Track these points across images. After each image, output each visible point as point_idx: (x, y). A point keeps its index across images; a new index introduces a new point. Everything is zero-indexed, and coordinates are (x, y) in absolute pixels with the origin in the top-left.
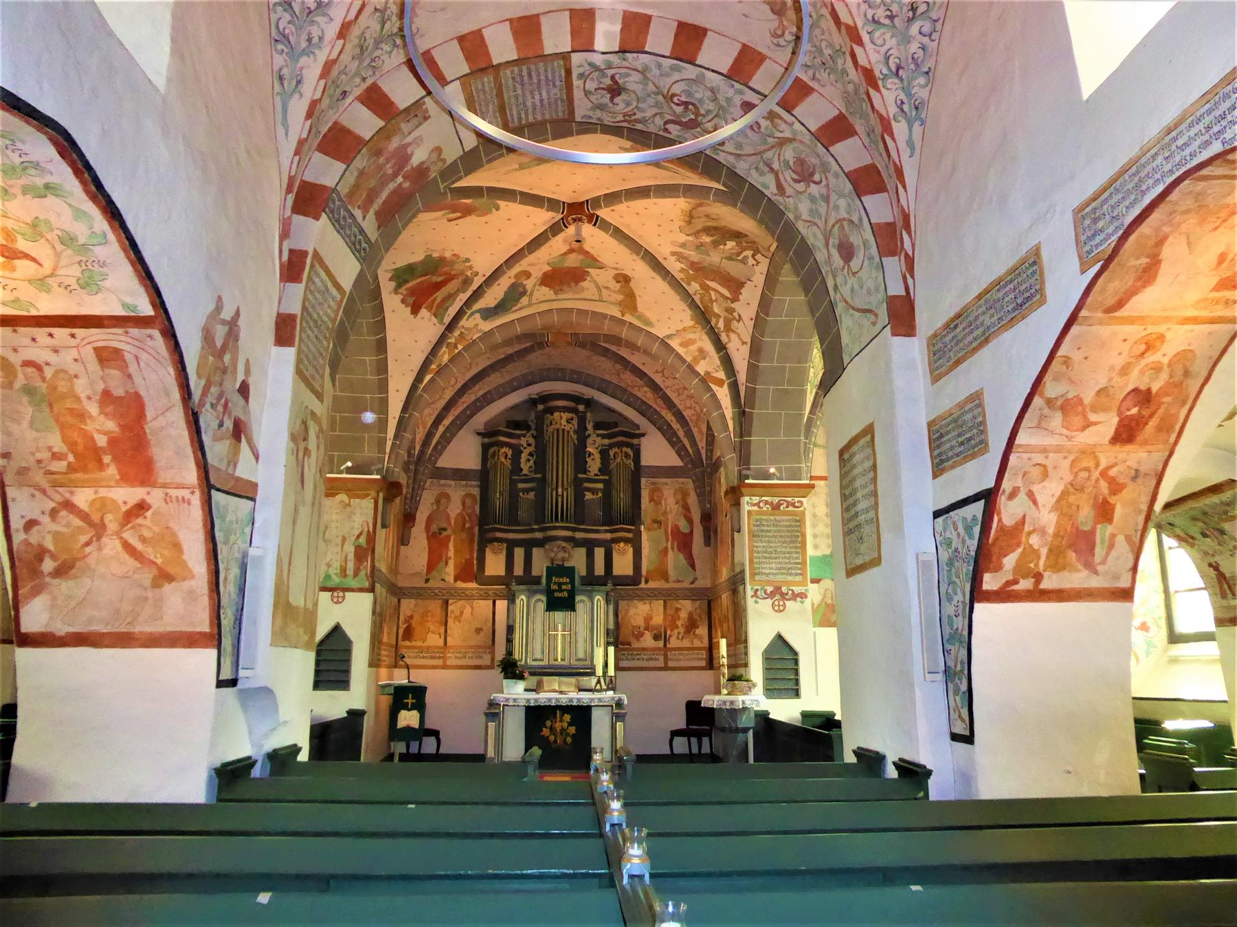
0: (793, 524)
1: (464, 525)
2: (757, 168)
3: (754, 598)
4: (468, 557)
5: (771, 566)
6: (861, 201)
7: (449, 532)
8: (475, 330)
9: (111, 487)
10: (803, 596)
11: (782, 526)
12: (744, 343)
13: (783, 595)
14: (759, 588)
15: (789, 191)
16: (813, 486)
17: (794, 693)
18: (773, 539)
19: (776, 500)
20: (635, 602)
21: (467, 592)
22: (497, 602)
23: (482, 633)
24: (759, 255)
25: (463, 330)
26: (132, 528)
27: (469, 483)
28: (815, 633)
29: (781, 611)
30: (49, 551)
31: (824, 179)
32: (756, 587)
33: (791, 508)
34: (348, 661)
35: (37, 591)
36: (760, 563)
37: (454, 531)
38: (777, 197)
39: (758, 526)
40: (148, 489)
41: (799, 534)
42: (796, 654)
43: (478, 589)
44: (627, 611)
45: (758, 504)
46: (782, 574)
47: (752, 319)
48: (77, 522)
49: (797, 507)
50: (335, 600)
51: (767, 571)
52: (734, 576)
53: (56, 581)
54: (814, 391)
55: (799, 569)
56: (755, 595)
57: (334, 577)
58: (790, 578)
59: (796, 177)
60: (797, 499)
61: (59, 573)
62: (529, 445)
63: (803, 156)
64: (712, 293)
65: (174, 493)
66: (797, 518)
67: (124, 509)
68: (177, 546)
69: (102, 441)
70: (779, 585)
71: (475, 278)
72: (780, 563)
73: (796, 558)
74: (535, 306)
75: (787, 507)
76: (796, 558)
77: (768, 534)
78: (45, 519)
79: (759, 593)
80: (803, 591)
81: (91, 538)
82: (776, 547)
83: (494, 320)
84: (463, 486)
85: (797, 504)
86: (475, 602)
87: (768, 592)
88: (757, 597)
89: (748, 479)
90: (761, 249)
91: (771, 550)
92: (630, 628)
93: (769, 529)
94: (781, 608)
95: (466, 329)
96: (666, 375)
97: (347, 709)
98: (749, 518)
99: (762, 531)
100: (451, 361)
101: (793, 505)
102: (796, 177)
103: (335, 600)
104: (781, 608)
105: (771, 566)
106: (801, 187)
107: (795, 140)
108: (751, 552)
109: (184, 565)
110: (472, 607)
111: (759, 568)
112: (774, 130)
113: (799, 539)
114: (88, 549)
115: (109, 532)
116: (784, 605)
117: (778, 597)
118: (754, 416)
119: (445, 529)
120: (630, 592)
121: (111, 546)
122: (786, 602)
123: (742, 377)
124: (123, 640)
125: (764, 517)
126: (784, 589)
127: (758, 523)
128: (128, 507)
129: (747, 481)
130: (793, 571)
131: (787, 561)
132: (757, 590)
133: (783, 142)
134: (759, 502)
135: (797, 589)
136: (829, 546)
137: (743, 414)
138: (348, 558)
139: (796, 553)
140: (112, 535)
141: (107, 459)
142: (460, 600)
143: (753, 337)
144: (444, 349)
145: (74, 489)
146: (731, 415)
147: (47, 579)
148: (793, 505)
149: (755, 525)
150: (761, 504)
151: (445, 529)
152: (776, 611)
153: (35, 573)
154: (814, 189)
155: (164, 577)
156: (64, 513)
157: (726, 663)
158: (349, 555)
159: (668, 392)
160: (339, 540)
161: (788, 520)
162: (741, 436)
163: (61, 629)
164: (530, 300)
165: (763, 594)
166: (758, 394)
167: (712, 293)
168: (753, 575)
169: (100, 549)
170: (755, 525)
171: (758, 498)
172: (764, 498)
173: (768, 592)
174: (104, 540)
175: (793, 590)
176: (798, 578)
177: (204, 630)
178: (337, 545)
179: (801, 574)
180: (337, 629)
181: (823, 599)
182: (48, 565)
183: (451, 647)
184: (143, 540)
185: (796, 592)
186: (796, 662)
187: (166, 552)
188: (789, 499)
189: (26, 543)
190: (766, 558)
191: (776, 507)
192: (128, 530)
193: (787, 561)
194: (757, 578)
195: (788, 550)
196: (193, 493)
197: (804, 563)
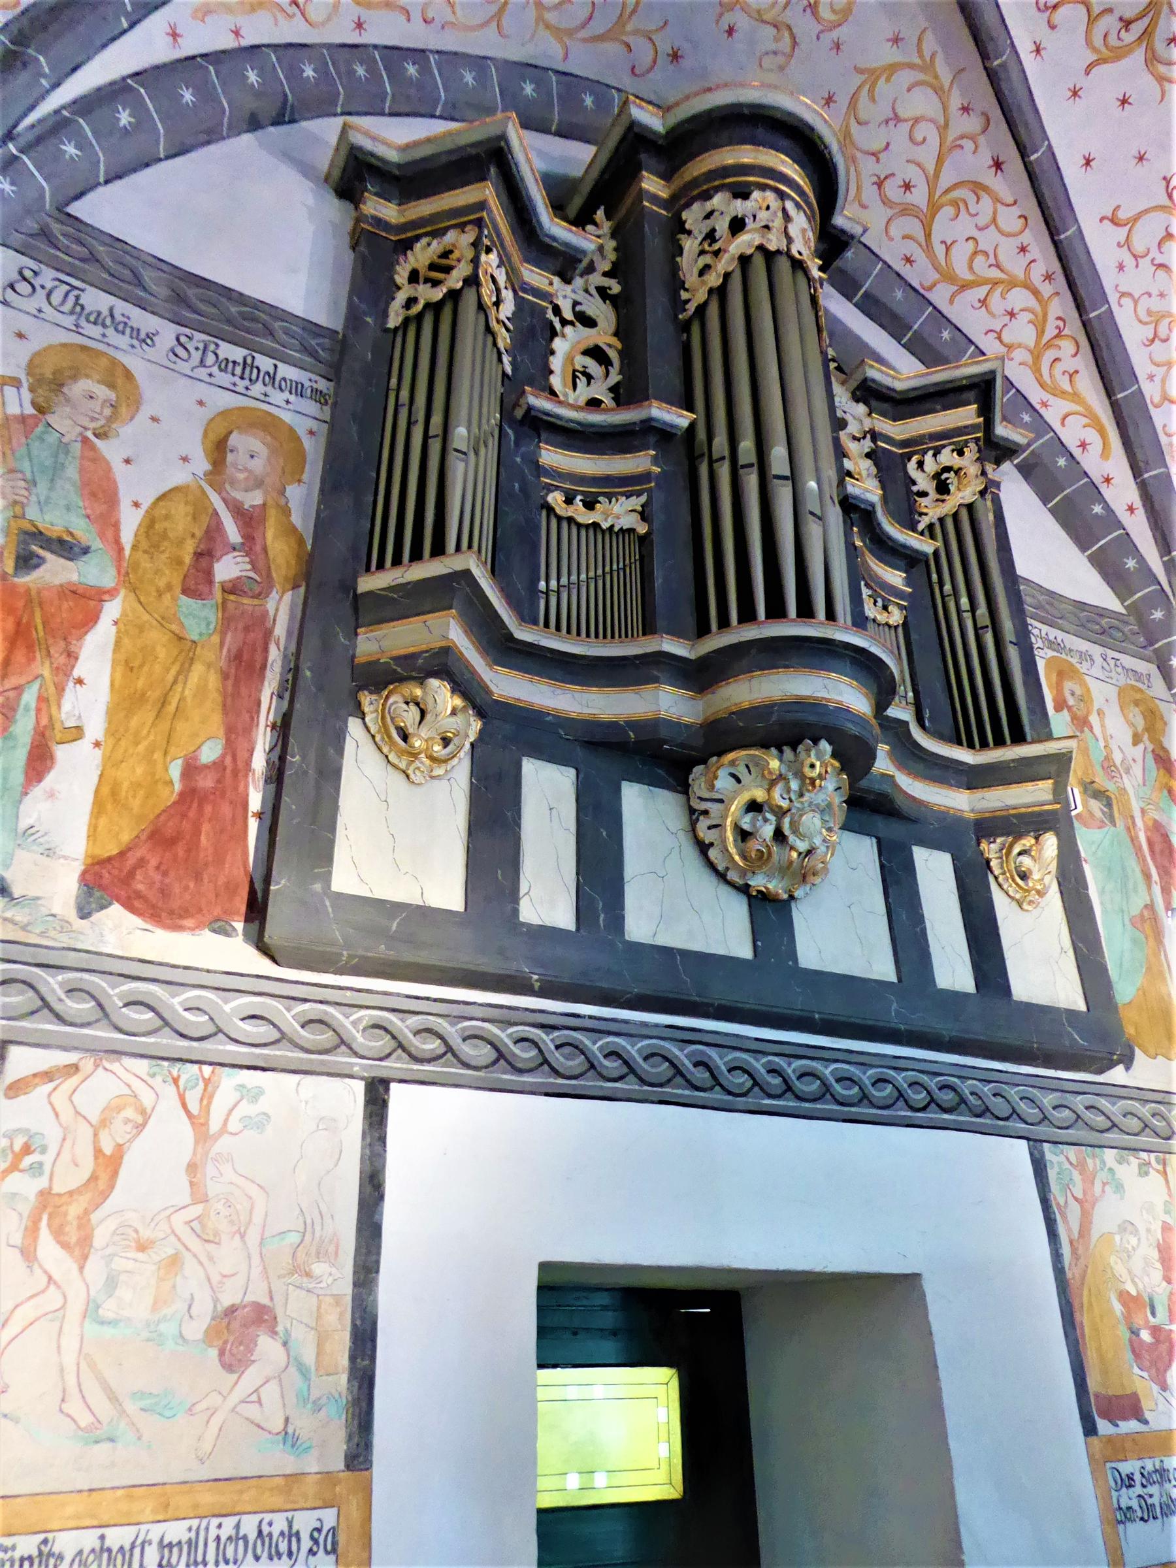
1: (205, 556)
4: (210, 753)
20: (1109, 1155)
21: (175, 1002)
22: (398, 1094)
23: (267, 1347)
27: (265, 363)
37: (129, 578)
43: (255, 986)
44: (1086, 1206)
62: (588, 322)
84: (225, 365)
86: (230, 1080)
92: (1118, 1308)
96: (1139, 246)
110: (198, 1122)
119: (68, 548)
120: (1079, 1102)
142: (118, 1053)
151: (68, 548)
159: (1124, 317)
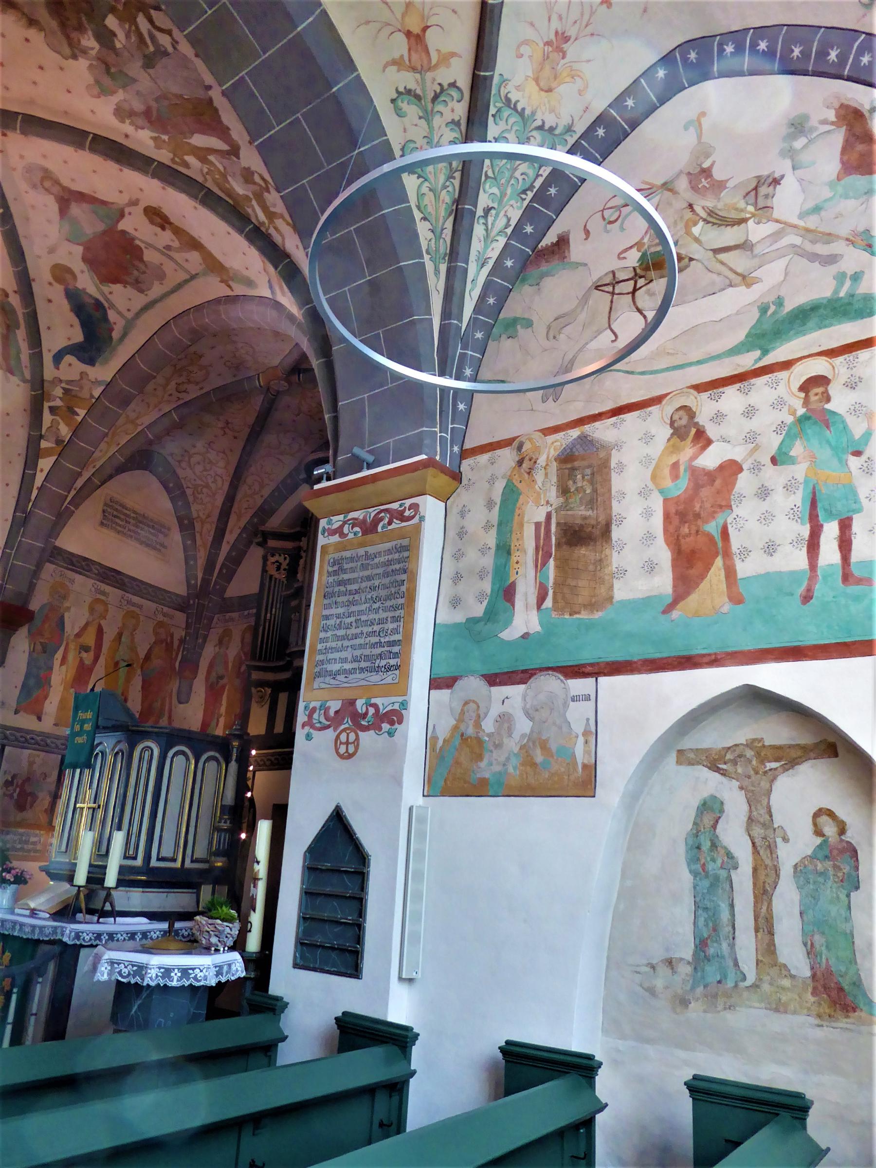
0: (396, 556)
5: (343, 655)
7: (225, 681)
8: (84, 381)
13: (357, 717)
25: (63, 385)
29: (350, 756)
32: (311, 706)
33: (396, 524)
39: (335, 573)
41: (404, 577)
46: (362, 670)
51: (336, 667)
54: (443, 268)
55: (396, 655)
60: (408, 502)
64: (212, 158)
66: (405, 542)
70: (350, 695)
71: (10, 299)
72: (361, 646)
73: (396, 631)
74: (140, 322)
75: (390, 523)
79: (316, 716)
82: (361, 612)
83: (106, 362)
85: (407, 513)
87: (332, 713)
88: (313, 727)
91: (349, 620)
93: (355, 575)
94: (351, 749)
95: (69, 382)
100: (74, 433)
105: (343, 655)
113: (404, 588)
117: (347, 723)
122: (360, 734)
125: (347, 554)
126: (360, 706)
130: (383, 663)
131: (374, 640)
132: (314, 710)
135: (384, 703)
136: (480, 598)
139: (396, 619)
144: (47, 417)
152: (342, 757)
161: (389, 552)
164: (119, 313)
165: (323, 720)
167: (212, 158)
170: (329, 574)
171: (341, 517)
172: (352, 515)
175: (375, 706)
181: (456, 728)
185: (382, 711)
188: (395, 506)
191: (369, 528)
193: (374, 640)
195: (383, 615)
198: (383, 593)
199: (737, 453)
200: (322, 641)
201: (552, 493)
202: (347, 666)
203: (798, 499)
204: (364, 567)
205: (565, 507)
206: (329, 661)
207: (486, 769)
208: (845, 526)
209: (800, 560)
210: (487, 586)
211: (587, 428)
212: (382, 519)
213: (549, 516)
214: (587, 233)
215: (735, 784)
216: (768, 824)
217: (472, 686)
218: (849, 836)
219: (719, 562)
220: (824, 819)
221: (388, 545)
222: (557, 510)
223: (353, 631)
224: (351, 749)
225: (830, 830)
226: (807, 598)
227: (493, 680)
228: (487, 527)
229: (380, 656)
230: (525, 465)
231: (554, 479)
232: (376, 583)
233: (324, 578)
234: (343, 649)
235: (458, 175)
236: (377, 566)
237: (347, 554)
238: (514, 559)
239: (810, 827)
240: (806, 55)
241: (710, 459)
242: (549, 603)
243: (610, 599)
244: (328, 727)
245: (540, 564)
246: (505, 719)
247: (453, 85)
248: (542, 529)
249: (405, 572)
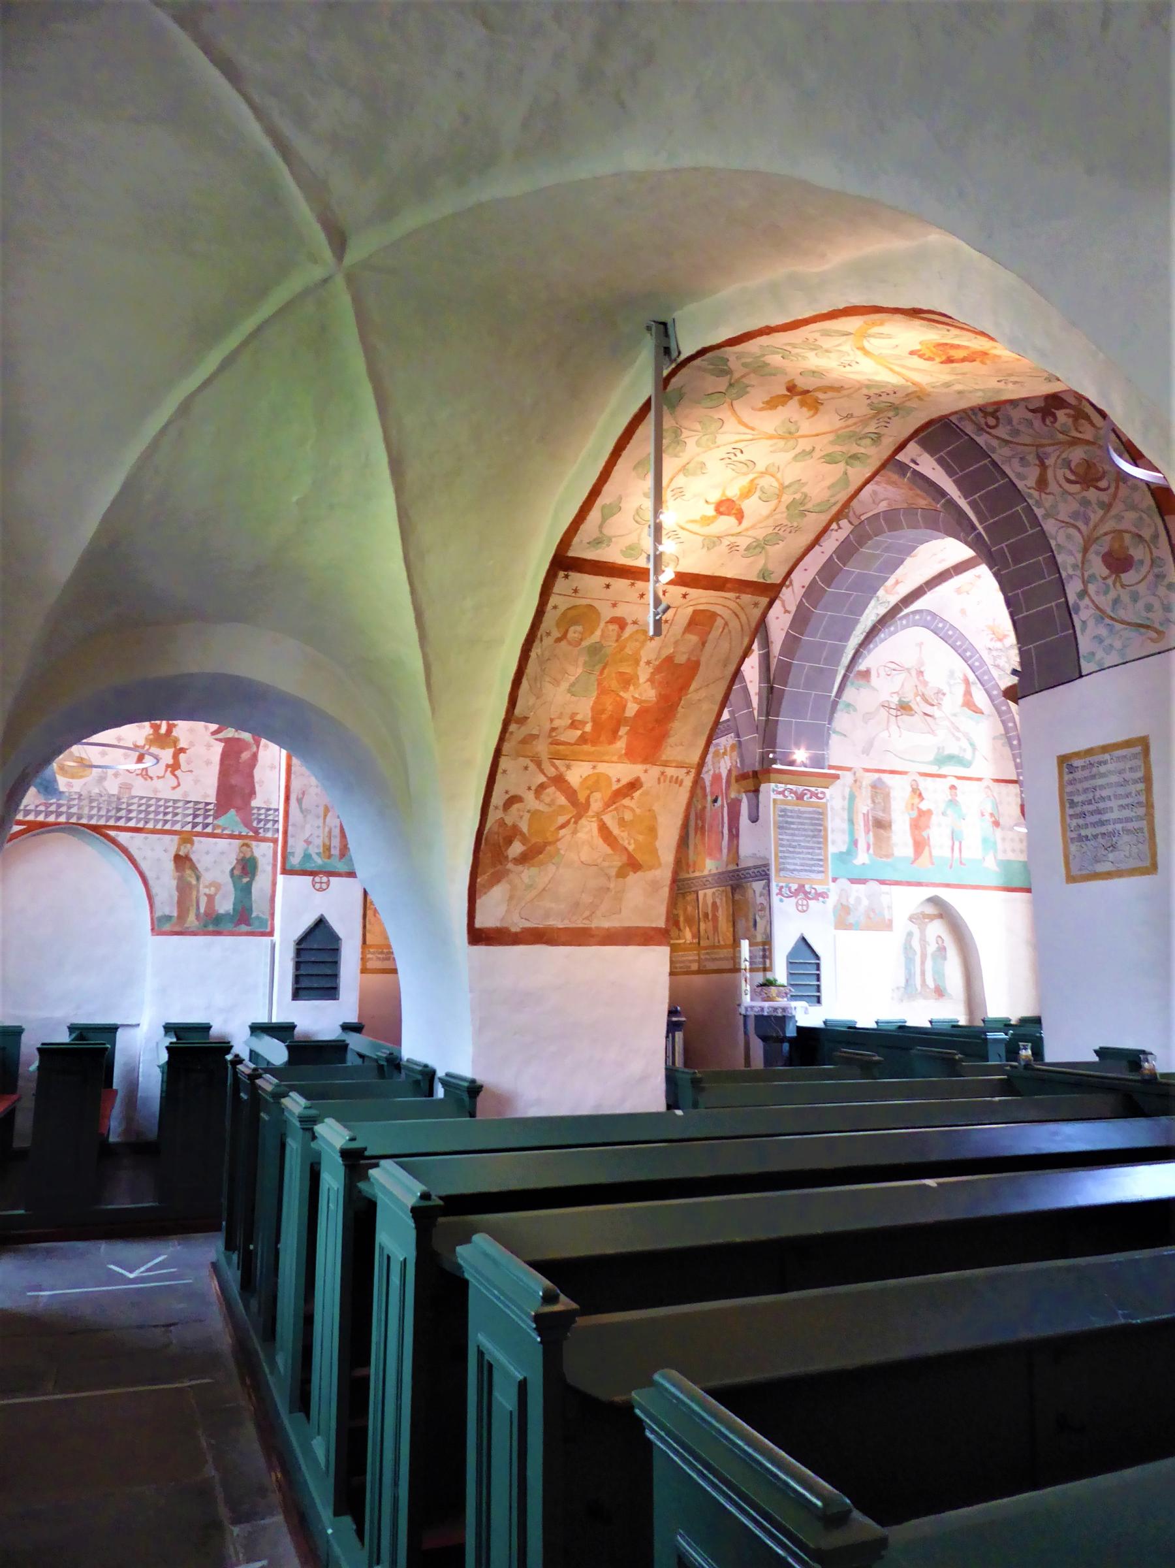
2: (1022, 459)
3: (780, 896)
6: (1163, 520)
9: (612, 762)
10: (824, 895)
11: (806, 818)
12: (786, 611)
13: (806, 893)
14: (784, 884)
15: (1053, 487)
16: (837, 777)
17: (816, 999)
18: (796, 832)
19: (800, 789)
24: (846, 520)
26: (616, 809)
28: (835, 936)
29: (804, 911)
30: (522, 834)
31: (1112, 490)
32: (781, 884)
33: (814, 799)
34: (336, 963)
35: (496, 879)
36: (785, 857)
38: (1032, 491)
40: (648, 766)
41: (821, 828)
42: (817, 957)
45: (782, 793)
46: (806, 870)
47: (803, 587)
48: (562, 800)
49: (821, 799)
50: (318, 886)
51: (792, 867)
52: (737, 870)
53: (520, 868)
55: (821, 866)
56: (780, 893)
57: (315, 857)
58: (813, 876)
59: (1073, 478)
60: (820, 790)
61: (523, 859)
63: (1095, 461)
65: (670, 771)
66: (820, 810)
67: (615, 787)
68: (652, 831)
69: (631, 709)
70: (802, 883)
72: (804, 859)
73: (819, 854)
75: (811, 798)
76: (819, 854)
77: (792, 826)
78: (529, 797)
79: (783, 890)
80: (825, 891)
81: (571, 818)
82: (800, 841)
85: (820, 795)
87: (793, 890)
89: (775, 763)
90: (851, 514)
91: (794, 844)
97: (341, 1023)
98: (774, 807)
99: (787, 822)
101: (816, 796)
102: (1073, 478)
103: (318, 886)
104: (805, 908)
106: (1076, 488)
107: (1093, 443)
108: (777, 845)
109: (654, 852)
111: (784, 863)
112: (1073, 428)
113: (822, 833)
114: (562, 832)
115: (590, 813)
116: (808, 906)
117: (801, 896)
118: (786, 693)
121: (588, 829)
122: (810, 902)
123: (776, 648)
124: (579, 937)
126: (807, 888)
127: (783, 813)
128: (620, 785)
129: (774, 766)
131: (810, 856)
132: (782, 888)
133: (1075, 442)
134: (784, 791)
135: (820, 888)
137: (771, 689)
138: (333, 834)
139: (820, 848)
140: (593, 817)
141: (623, 731)
143: (800, 605)
145: (572, 762)
146: (757, 690)
147: (510, 866)
148: (816, 796)
149: (780, 816)
150: (787, 793)
153: (499, 856)
154: (1092, 494)
155: (633, 865)
156: (551, 790)
157: (748, 967)
158: (333, 829)
160: (321, 810)
162: (768, 714)
163: (517, 924)
166: (793, 670)
168: (779, 870)
169: (574, 832)
170: (780, 816)
171: (783, 785)
172: (789, 786)
173: (793, 890)
174: (583, 821)
176: (820, 876)
177: (659, 926)
178: (318, 817)
179: (822, 872)
180: (321, 923)
181: (838, 900)
182: (516, 849)
183: (370, 946)
184: (622, 822)
186: (818, 966)
187: (640, 838)
188: (813, 789)
189: (502, 823)
190: (790, 852)
192: (611, 811)
193: (810, 856)
194: (782, 874)
195: (811, 845)
196: (688, 773)
197: (825, 860)
198: (811, 833)
199: (932, 807)
200: (782, 852)
201: (869, 802)
202: (798, 868)
203: (949, 832)
204: (799, 817)
205: (873, 809)
206: (788, 863)
207: (851, 919)
208: (960, 843)
209: (949, 855)
210: (846, 838)
211: (886, 778)
212: (806, 794)
213: (868, 812)
214: (878, 674)
215: (917, 926)
216: (925, 941)
217: (843, 883)
218: (945, 945)
219: (927, 848)
220: (939, 939)
221: (811, 809)
222: (872, 809)
223: (797, 850)
224: (800, 908)
225: (940, 942)
226: (951, 867)
227: (853, 881)
228: (843, 809)
229: (814, 865)
230: (858, 783)
231: (869, 795)
232: (806, 827)
233: (777, 816)
234: (794, 858)
235: (865, 634)
236: (806, 818)
237: (789, 808)
238: (856, 827)
239: (935, 942)
240: (961, 646)
241: (924, 806)
242: (871, 851)
243: (893, 854)
244: (791, 897)
245: (867, 832)
246: (858, 900)
247: (889, 602)
248: (866, 816)
249: (821, 825)
